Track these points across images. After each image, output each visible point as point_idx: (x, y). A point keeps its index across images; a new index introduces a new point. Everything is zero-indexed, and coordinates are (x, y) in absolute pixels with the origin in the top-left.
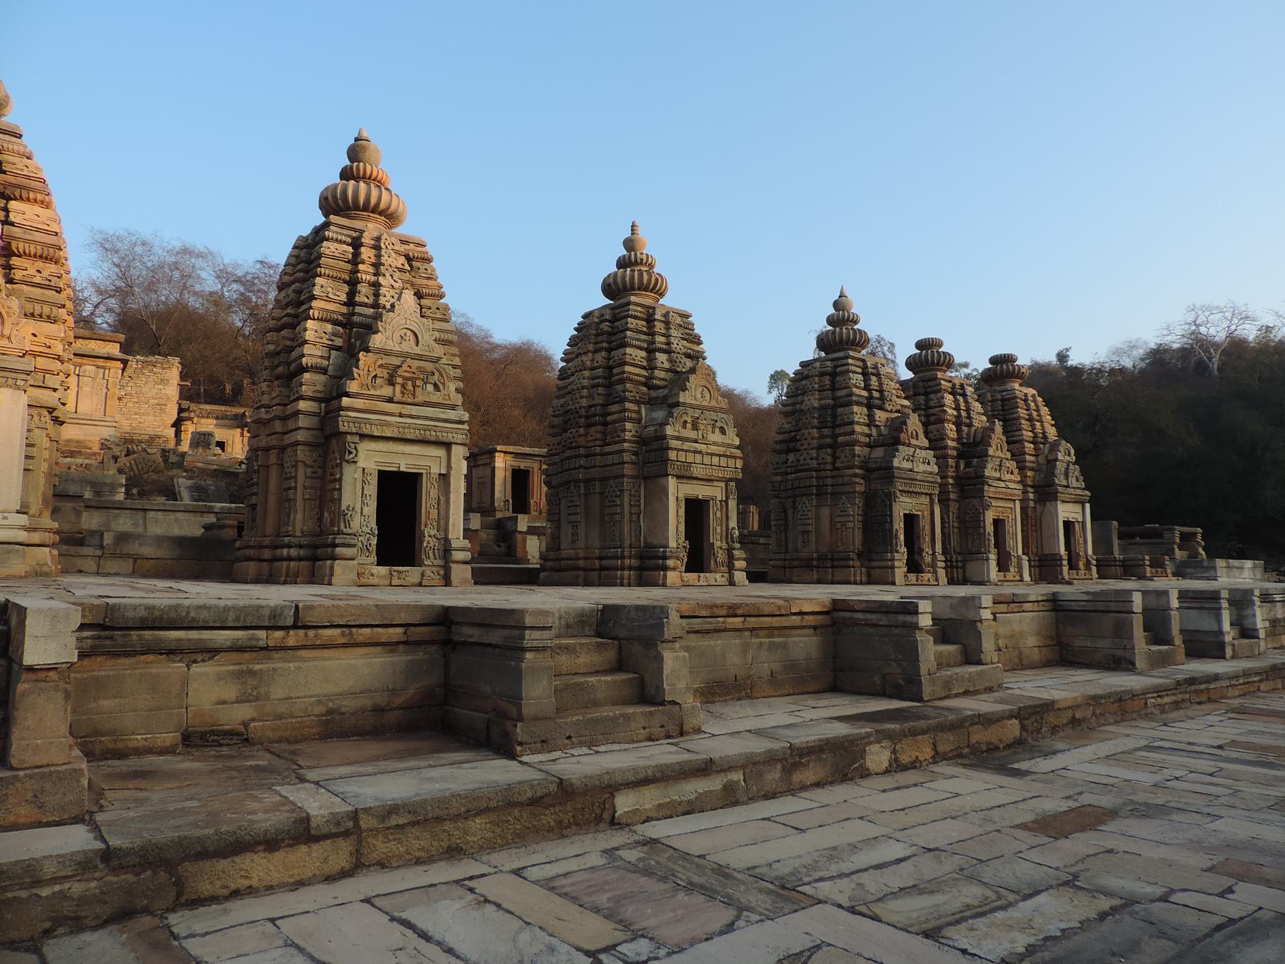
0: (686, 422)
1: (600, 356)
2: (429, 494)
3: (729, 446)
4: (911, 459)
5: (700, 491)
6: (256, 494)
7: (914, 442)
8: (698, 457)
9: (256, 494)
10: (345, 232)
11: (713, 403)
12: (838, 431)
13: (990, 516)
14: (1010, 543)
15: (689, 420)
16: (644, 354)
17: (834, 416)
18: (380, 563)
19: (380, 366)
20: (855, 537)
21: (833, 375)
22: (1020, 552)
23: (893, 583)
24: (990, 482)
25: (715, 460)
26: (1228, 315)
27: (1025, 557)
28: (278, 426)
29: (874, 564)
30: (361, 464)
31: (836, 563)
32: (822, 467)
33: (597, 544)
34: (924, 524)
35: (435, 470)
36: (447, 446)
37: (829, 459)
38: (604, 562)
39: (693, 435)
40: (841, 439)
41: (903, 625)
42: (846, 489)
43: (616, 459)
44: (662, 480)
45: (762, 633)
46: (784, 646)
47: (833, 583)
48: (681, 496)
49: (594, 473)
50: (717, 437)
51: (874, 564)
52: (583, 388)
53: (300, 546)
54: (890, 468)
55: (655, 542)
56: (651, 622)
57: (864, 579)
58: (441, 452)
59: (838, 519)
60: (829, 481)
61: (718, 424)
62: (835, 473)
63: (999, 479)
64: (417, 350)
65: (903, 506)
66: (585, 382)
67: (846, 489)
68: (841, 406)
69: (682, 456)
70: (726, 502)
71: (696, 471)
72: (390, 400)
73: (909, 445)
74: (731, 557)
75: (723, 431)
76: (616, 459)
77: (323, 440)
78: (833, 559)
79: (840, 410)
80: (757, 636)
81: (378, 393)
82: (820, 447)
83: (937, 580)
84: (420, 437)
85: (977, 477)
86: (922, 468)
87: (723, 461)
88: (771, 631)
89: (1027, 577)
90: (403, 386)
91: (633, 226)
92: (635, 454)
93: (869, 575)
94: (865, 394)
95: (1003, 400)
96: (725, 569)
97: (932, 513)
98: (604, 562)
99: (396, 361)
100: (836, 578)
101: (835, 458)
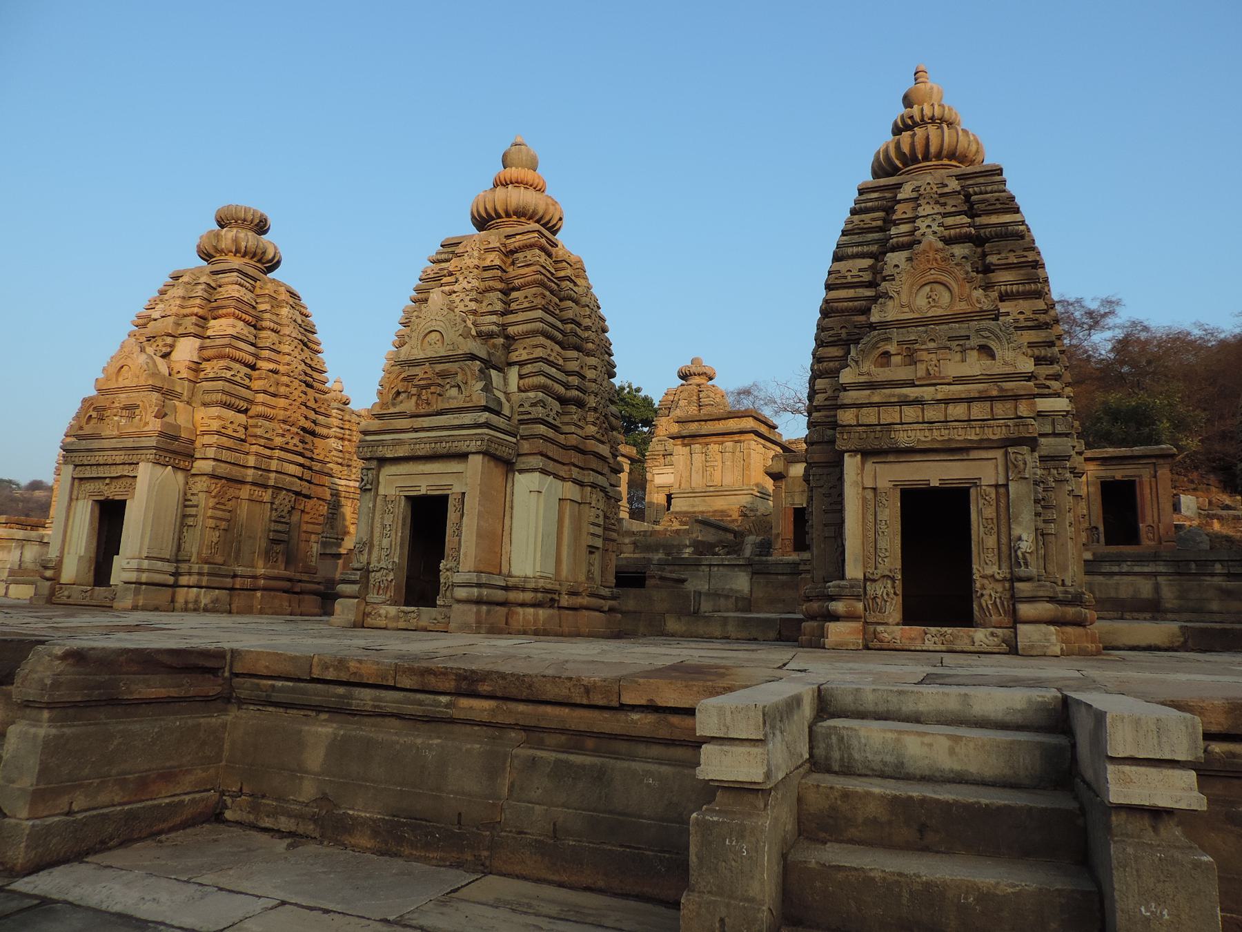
0: (886, 354)
8: (910, 413)
11: (961, 307)
15: (892, 348)
19: (404, 379)
25: (958, 411)
30: (382, 491)
39: (903, 373)
45: (550, 739)
46: (599, 776)
48: (883, 484)
50: (975, 365)
61: (975, 341)
69: (869, 416)
70: (1006, 486)
71: (904, 438)
80: (540, 745)
81: (396, 410)
84: (430, 453)
87: (978, 411)
88: (576, 739)
96: (1006, 620)
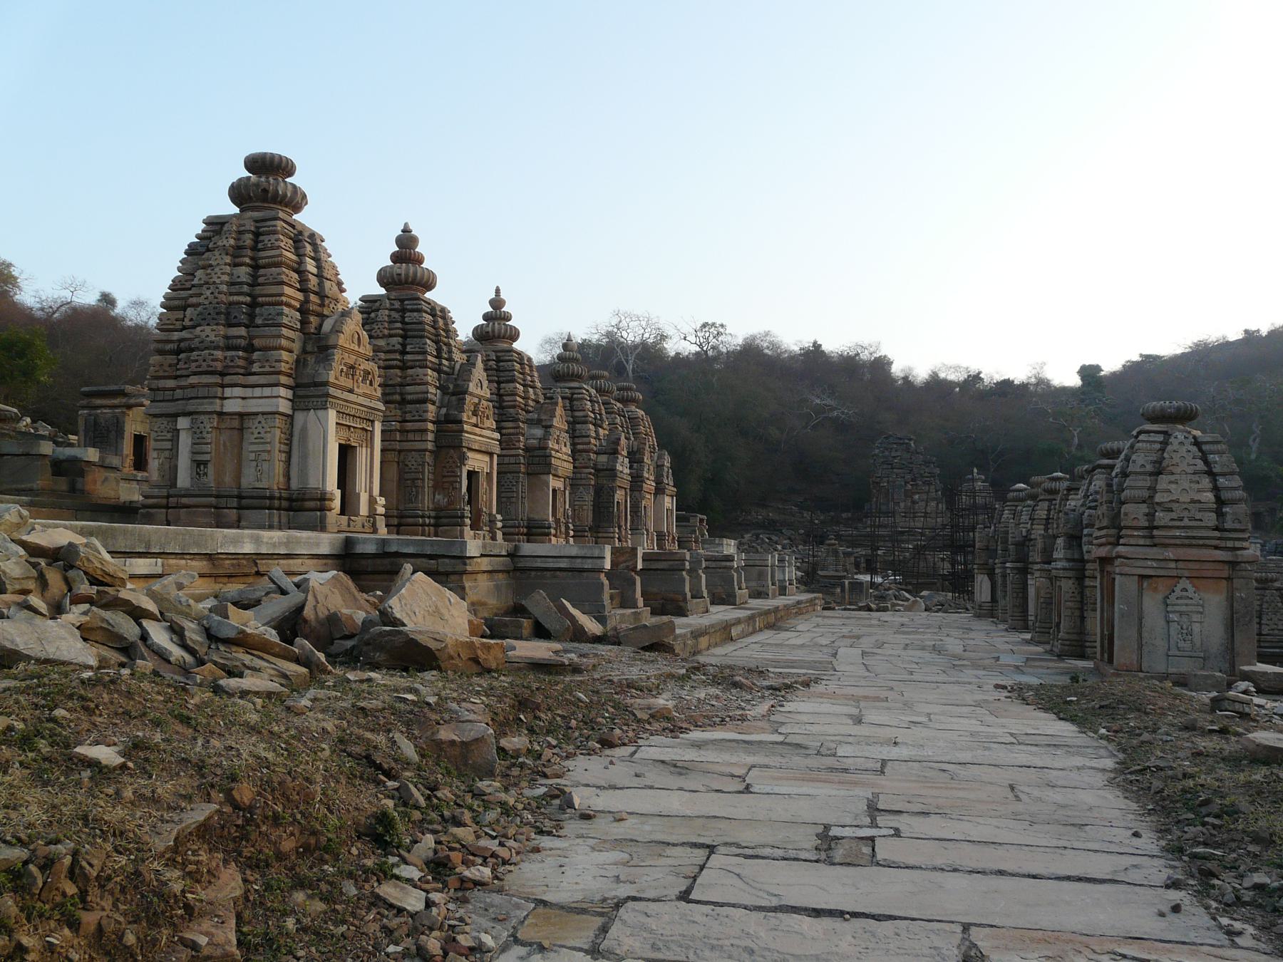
26: (644, 323)
34: (622, 507)
41: (725, 567)
42: (583, 482)
43: (512, 460)
44: (544, 477)
54: (613, 470)
55: (536, 517)
58: (487, 458)
67: (583, 482)
74: (567, 528)
76: (512, 460)
91: (498, 291)
99: (476, 400)
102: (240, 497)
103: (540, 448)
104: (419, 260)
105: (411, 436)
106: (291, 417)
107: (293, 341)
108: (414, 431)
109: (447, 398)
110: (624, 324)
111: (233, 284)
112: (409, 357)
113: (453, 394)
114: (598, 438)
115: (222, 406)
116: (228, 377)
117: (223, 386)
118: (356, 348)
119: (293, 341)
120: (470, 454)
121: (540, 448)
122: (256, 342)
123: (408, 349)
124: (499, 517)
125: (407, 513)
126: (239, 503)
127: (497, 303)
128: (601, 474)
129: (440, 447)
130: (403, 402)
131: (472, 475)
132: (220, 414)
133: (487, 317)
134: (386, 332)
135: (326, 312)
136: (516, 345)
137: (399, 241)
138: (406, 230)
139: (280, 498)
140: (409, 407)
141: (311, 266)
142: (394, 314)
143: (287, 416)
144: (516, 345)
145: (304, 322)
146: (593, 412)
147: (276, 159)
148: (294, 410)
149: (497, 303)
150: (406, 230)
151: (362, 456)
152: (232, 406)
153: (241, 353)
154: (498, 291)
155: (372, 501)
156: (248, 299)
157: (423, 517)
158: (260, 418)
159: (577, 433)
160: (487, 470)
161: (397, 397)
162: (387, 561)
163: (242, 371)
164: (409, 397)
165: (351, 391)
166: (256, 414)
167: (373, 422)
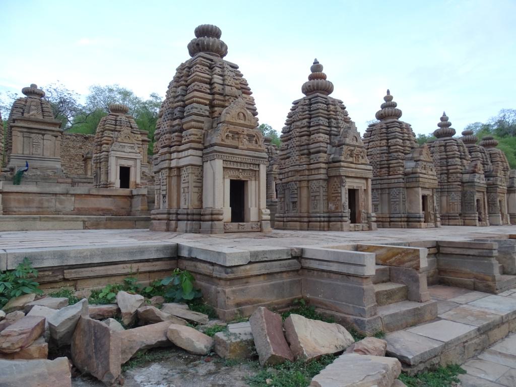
1: (384, 142)
2: (361, 196)
3: (433, 175)
4: (479, 178)
5: (427, 193)
6: (297, 197)
7: (480, 172)
9: (297, 197)
10: (324, 99)
11: (429, 160)
12: (449, 167)
13: (498, 199)
14: (503, 209)
16: (402, 141)
17: (447, 162)
18: (351, 223)
20: (458, 208)
21: (445, 146)
22: (506, 213)
23: (476, 226)
24: (499, 187)
27: (508, 215)
28: (307, 173)
29: (467, 218)
31: (450, 218)
32: (443, 181)
33: (387, 212)
34: (482, 202)
35: (363, 188)
36: (366, 179)
37: (446, 178)
38: (392, 219)
40: (451, 171)
44: (416, 189)
47: (449, 225)
49: (385, 186)
50: (430, 173)
51: (467, 218)
52: (378, 154)
53: (324, 217)
55: (413, 212)
56: (505, 245)
57: (463, 223)
58: (364, 181)
59: (451, 201)
60: (446, 187)
61: (431, 168)
62: (449, 184)
63: (501, 185)
64: (357, 144)
65: (477, 196)
66: (378, 152)
68: (450, 158)
72: (352, 163)
73: (478, 173)
74: (436, 217)
75: (432, 170)
77: (327, 178)
78: (449, 216)
79: (450, 160)
82: (441, 174)
83: (487, 224)
85: (494, 185)
86: (482, 182)
89: (509, 223)
90: (355, 157)
91: (388, 92)
92: (403, 179)
93: (464, 222)
94: (459, 153)
95: (490, 154)
96: (433, 221)
97: (484, 199)
98: (392, 219)
99: (352, 148)
100: (450, 223)
101: (448, 178)
102: (177, 214)
103: (413, 173)
104: (324, 77)
105: (313, 172)
106: (202, 166)
107: (203, 122)
108: (315, 169)
109: (334, 148)
110: (507, 117)
111: (177, 96)
112: (311, 129)
113: (339, 146)
114: (463, 165)
115: (170, 163)
116: (172, 148)
117: (171, 153)
118: (242, 122)
119: (203, 122)
120: (347, 180)
121: (413, 173)
122: (185, 126)
123: (312, 124)
124: (373, 214)
125: (312, 215)
126: (177, 217)
127: (388, 98)
128: (465, 185)
129: (329, 179)
130: (309, 154)
131: (352, 193)
132: (170, 169)
133: (383, 107)
134: (300, 117)
135: (227, 104)
136: (400, 119)
137: (313, 69)
138: (316, 62)
139: (193, 214)
140: (312, 156)
141: (217, 79)
142: (306, 107)
143: (200, 166)
144: (400, 119)
145: (212, 112)
146: (459, 151)
147: (210, 29)
148: (203, 162)
149: (388, 98)
150: (316, 62)
151: (251, 187)
152: (174, 164)
153: (176, 134)
154: (388, 92)
155: (260, 213)
156: (182, 103)
157: (320, 217)
158: (185, 168)
159: (449, 164)
160: (364, 187)
161: (306, 151)
162: (193, 263)
163: (178, 143)
164: (312, 151)
165: (237, 148)
166: (183, 167)
167: (259, 165)
